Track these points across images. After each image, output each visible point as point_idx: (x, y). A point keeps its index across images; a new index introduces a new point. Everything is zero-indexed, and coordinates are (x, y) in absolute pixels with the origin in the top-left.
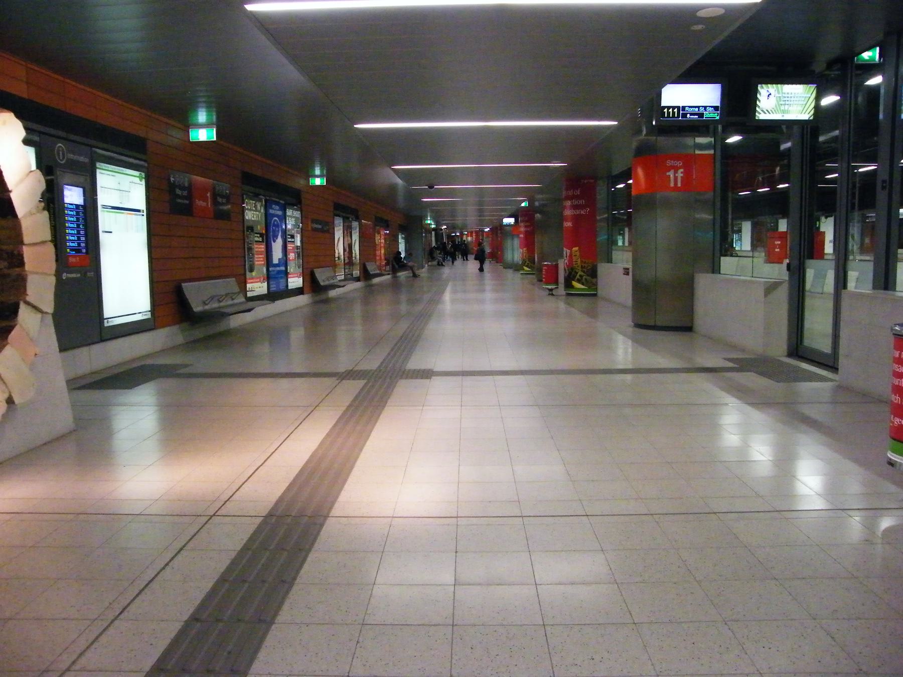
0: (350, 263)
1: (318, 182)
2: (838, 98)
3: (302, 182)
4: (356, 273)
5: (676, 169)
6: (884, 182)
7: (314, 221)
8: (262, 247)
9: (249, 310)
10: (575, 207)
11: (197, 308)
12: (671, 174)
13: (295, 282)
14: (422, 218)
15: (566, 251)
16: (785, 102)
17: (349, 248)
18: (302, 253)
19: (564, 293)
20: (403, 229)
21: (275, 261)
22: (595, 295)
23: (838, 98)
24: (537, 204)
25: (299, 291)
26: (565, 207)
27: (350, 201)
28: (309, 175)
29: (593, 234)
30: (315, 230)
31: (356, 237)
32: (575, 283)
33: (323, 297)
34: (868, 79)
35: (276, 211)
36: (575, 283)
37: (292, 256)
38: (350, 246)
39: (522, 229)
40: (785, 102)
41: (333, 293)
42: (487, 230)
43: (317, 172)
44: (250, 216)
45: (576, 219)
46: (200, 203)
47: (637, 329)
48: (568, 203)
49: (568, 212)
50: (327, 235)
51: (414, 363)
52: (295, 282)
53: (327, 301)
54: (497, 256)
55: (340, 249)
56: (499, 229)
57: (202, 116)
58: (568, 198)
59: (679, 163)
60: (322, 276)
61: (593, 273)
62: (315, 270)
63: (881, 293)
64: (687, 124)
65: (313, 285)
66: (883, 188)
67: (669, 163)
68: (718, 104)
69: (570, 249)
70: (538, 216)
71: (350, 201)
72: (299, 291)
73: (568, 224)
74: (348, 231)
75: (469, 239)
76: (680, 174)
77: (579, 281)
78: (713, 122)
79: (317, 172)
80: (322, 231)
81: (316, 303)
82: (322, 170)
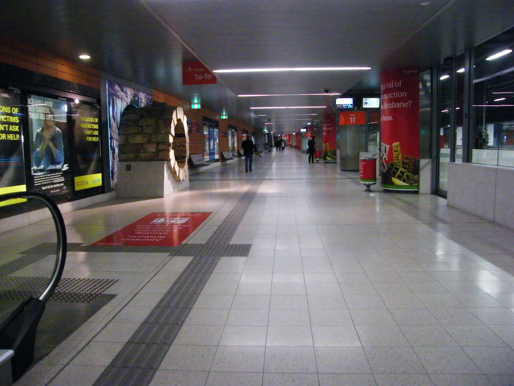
0: (233, 150)
1: (224, 117)
2: (448, 76)
3: (219, 117)
4: (236, 154)
5: (353, 117)
6: (466, 114)
7: (223, 133)
8: (207, 143)
9: (208, 165)
10: (328, 127)
11: (195, 163)
12: (351, 118)
13: (217, 157)
14: (262, 129)
15: (324, 145)
16: (372, 103)
17: (233, 144)
18: (219, 145)
19: (323, 162)
20: (254, 134)
21: (211, 149)
22: (335, 163)
23: (448, 76)
24: (315, 124)
25: (217, 160)
26: (323, 127)
27: (235, 124)
28: (221, 115)
29: (334, 137)
30: (222, 136)
31: (236, 138)
32: (328, 158)
33: (224, 163)
34: (487, 57)
35: (211, 130)
36: (328, 158)
37: (216, 147)
38: (234, 143)
39: (309, 134)
40: (372, 103)
41: (228, 162)
42: (294, 134)
43: (224, 113)
44: (206, 133)
45: (328, 132)
46: (193, 129)
47: (344, 172)
48: (325, 125)
49: (324, 129)
50: (225, 138)
51: (266, 178)
52: (217, 157)
53: (226, 165)
54: (298, 147)
55: (230, 144)
56: (299, 134)
57: (196, 101)
58: (325, 123)
59: (354, 115)
60: (226, 155)
61: (335, 154)
62: (223, 153)
63: (467, 164)
64: (344, 110)
65: (223, 159)
66: (466, 117)
67: (351, 115)
68: (352, 103)
69: (325, 143)
70: (315, 129)
71: (235, 124)
72: (217, 160)
73: (324, 134)
74: (233, 136)
75: (285, 138)
76: (354, 119)
77: (329, 157)
78: (350, 109)
79: (224, 113)
80: (225, 136)
81: (222, 165)
82: (226, 112)
